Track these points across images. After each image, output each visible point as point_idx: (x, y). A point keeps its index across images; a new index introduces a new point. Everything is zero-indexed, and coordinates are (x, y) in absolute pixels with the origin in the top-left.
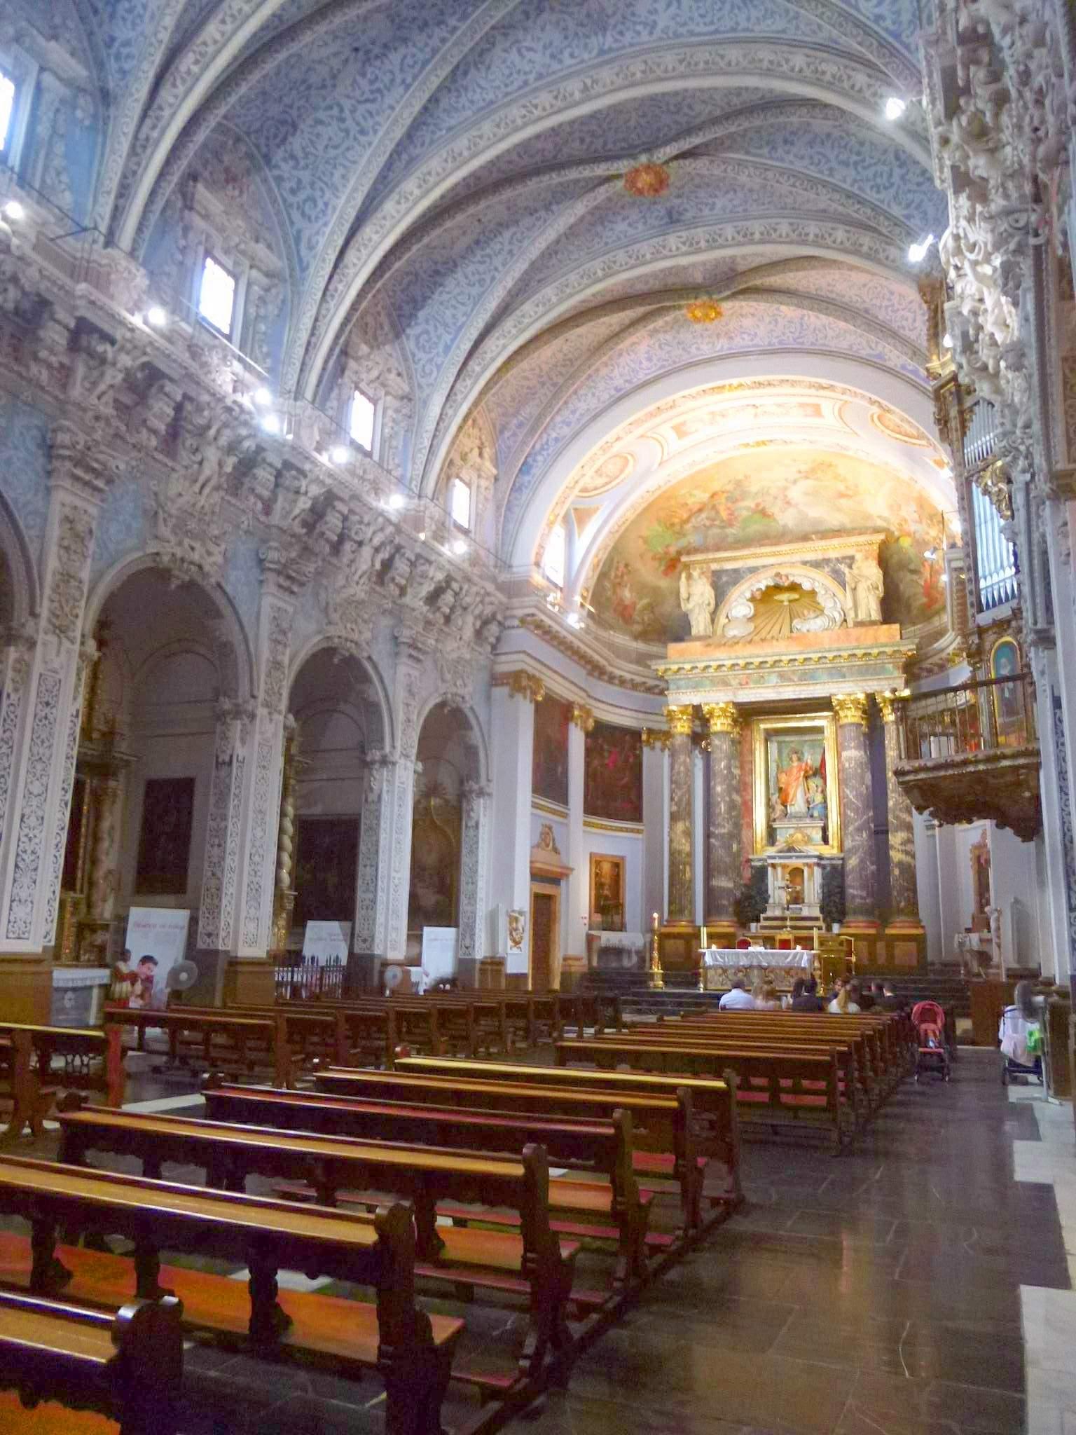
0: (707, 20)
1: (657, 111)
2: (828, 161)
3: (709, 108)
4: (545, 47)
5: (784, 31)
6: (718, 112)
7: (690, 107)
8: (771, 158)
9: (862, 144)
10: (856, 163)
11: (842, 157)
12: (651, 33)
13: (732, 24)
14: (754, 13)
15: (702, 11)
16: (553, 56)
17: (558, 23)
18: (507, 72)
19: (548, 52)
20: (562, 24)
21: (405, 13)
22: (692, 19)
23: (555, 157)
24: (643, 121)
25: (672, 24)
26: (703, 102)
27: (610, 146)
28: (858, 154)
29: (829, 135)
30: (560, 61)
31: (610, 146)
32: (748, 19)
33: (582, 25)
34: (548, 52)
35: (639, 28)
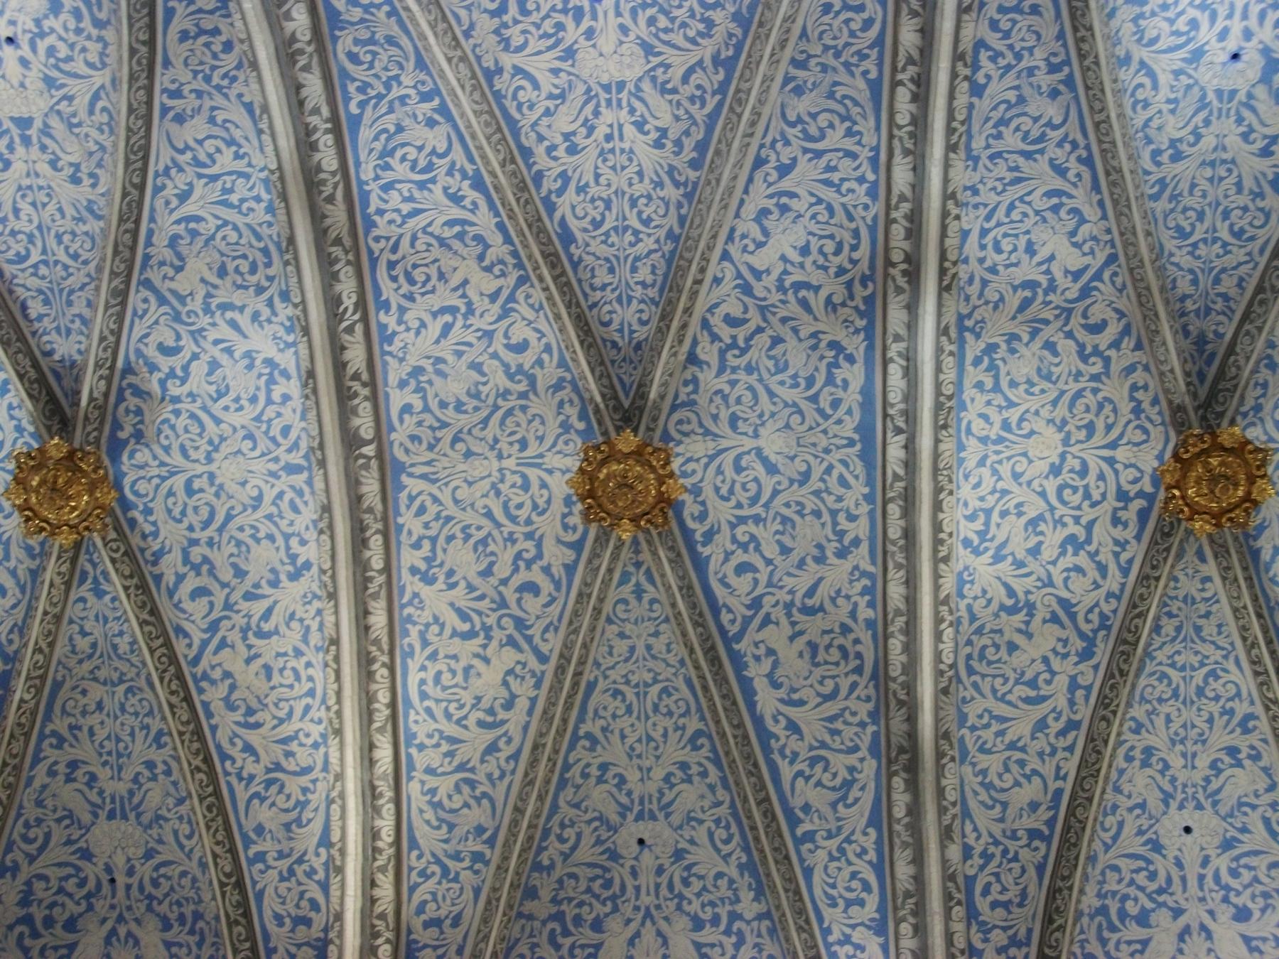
0: (429, 688)
1: (191, 518)
2: (32, 859)
3: (197, 636)
4: (439, 360)
5: (414, 844)
6: (180, 646)
7: (199, 593)
8: (42, 737)
9: (71, 925)
10: (28, 920)
11: (39, 886)
12: (414, 570)
13: (421, 738)
14: (445, 786)
15: (446, 679)
16: (418, 371)
17: (477, 396)
18: (419, 275)
19: (427, 364)
20: (471, 404)
21: (608, 116)
22: (433, 656)
23: (147, 284)
24: (178, 482)
25: (426, 616)
26: (214, 627)
27: (132, 402)
28: (49, 922)
29: (87, 855)
30: (402, 384)
31: (132, 402)
32: (430, 771)
33: (456, 439)
34: (427, 364)
35: (427, 545)
